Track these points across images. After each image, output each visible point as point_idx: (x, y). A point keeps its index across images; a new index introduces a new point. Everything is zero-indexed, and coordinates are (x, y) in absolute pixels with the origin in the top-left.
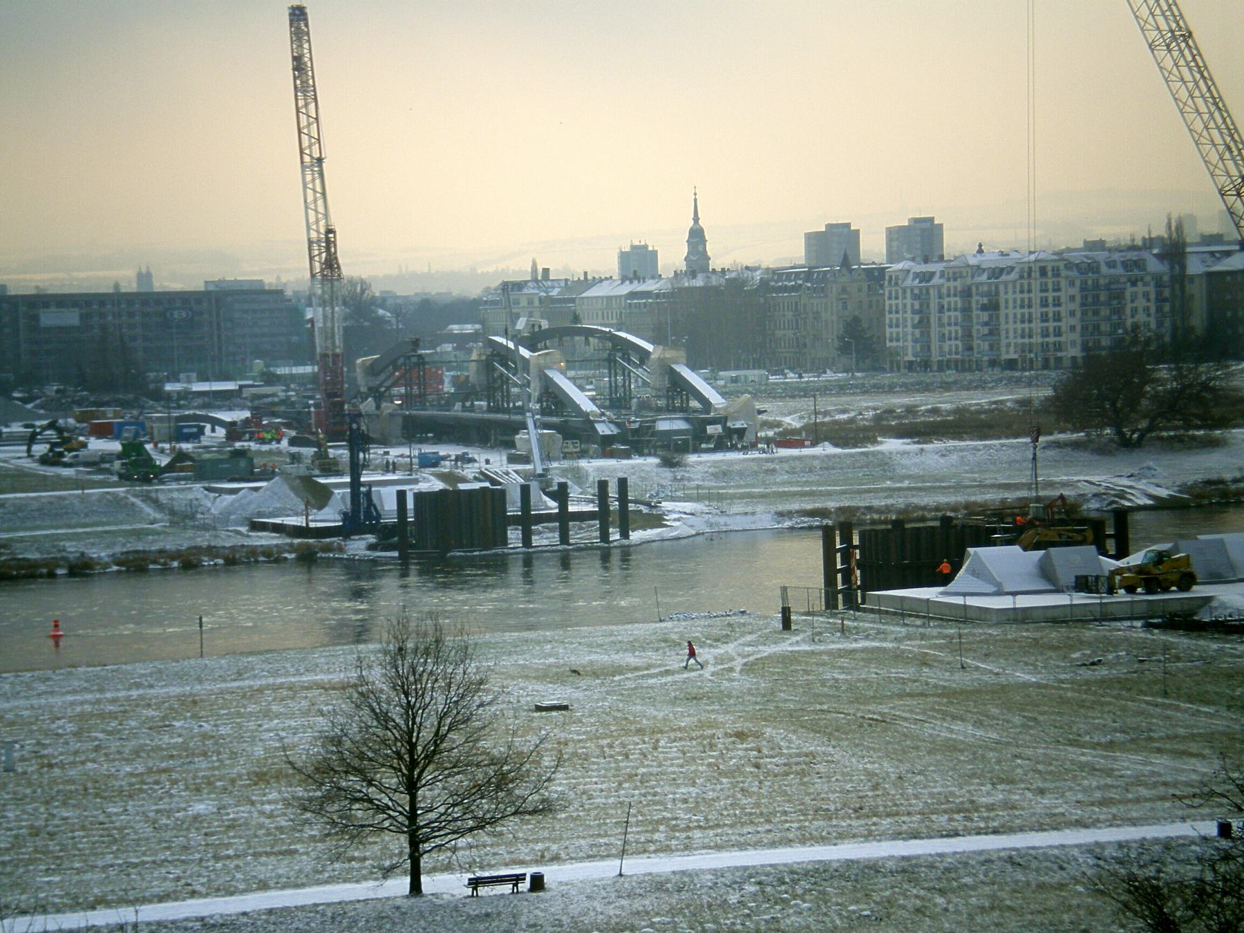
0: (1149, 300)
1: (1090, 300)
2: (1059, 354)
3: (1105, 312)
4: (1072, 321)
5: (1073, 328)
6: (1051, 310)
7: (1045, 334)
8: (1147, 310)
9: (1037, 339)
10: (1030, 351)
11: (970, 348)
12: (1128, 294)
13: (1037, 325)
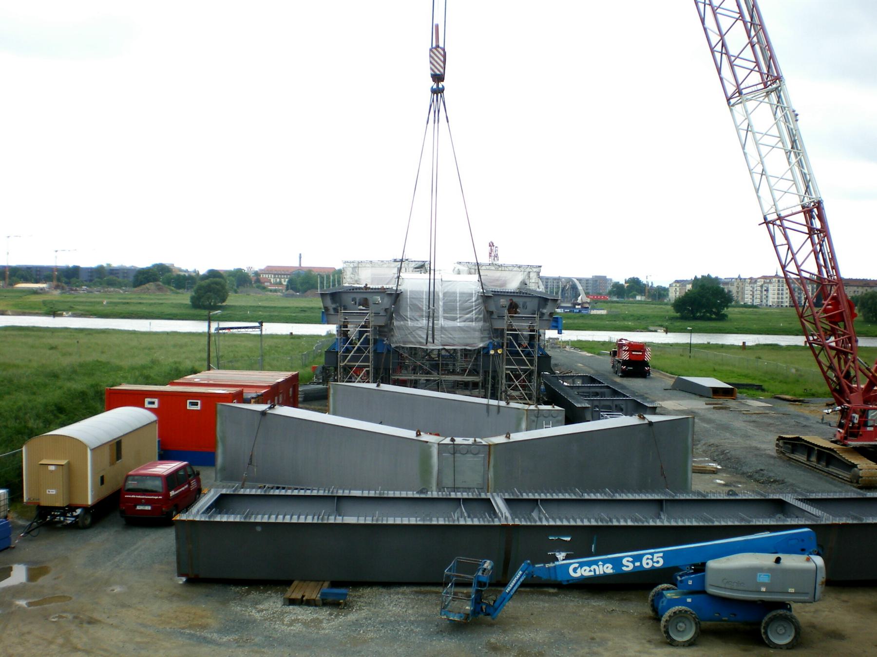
4: (787, 296)
5: (787, 297)
9: (776, 300)
11: (762, 302)
13: (776, 296)
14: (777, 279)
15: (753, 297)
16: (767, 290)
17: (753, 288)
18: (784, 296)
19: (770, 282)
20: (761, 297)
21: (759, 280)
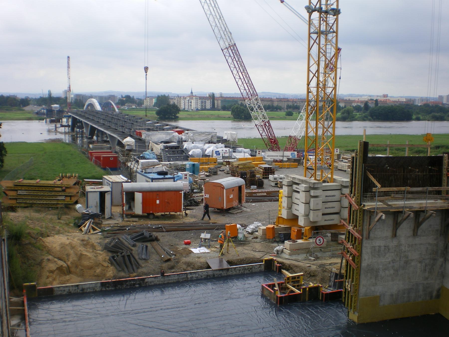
3: (204, 104)
6: (197, 103)
8: (209, 104)
9: (195, 107)
13: (195, 105)
14: (195, 98)
15: (185, 105)
16: (191, 102)
17: (185, 101)
18: (198, 105)
19: (192, 99)
21: (187, 98)
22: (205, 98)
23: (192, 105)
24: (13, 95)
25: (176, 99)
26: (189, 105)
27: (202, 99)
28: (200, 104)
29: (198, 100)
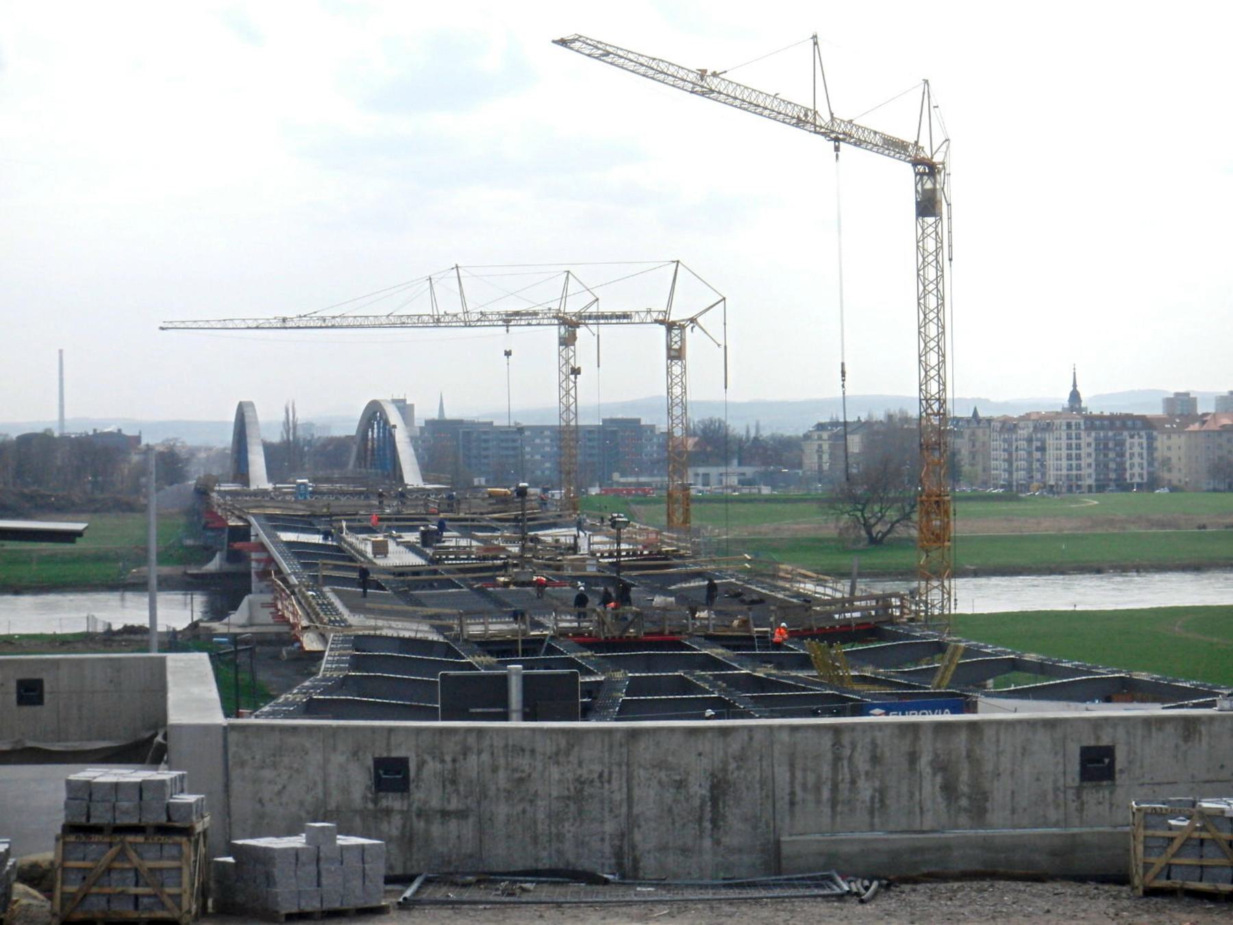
0: (1142, 448)
1: (1102, 446)
2: (1079, 483)
3: (1112, 455)
5: (1089, 465)
6: (1074, 452)
7: (1070, 468)
8: (1141, 455)
9: (1064, 472)
10: (1061, 480)
11: (1032, 477)
12: (1128, 445)
13: (1064, 463)
15: (1011, 464)
16: (1042, 449)
17: (1010, 445)
18: (1083, 463)
20: (1030, 464)
22: (1118, 423)
23: (1051, 462)
24: (112, 428)
25: (967, 432)
26: (1036, 465)
27: (1102, 428)
28: (1089, 455)
29: (1078, 437)
